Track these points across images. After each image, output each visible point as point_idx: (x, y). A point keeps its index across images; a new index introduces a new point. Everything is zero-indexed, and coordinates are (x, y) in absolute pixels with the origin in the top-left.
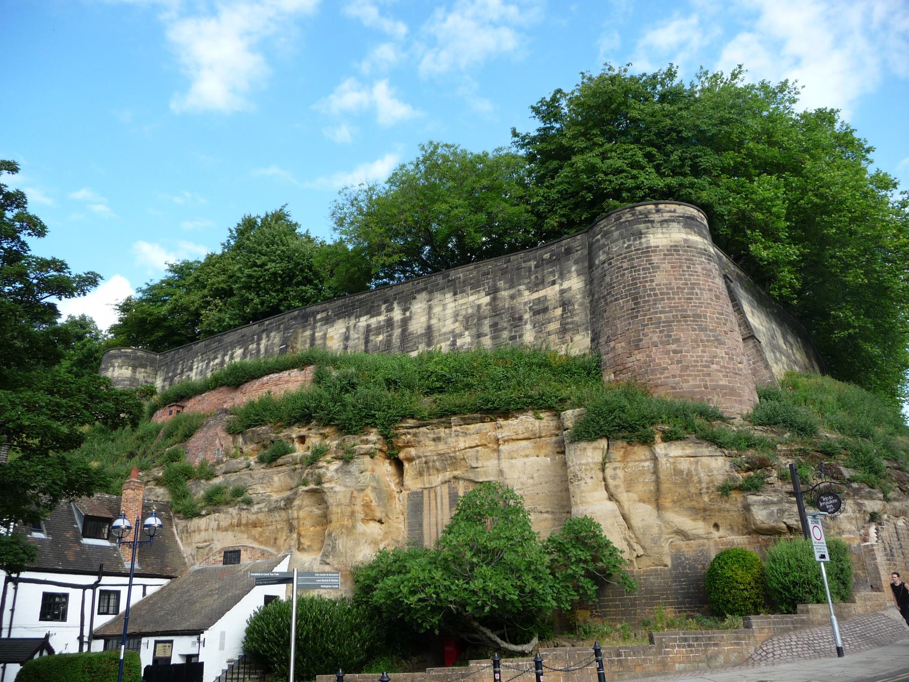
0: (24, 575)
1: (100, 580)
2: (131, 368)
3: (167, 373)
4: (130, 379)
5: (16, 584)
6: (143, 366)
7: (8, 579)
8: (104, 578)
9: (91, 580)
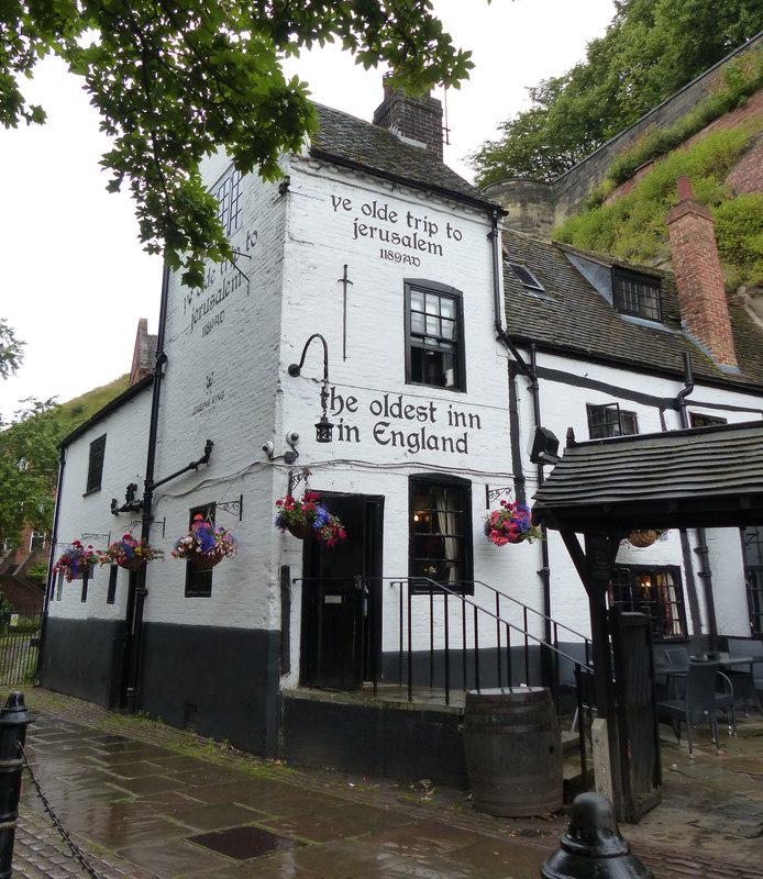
0: (544, 361)
1: (689, 392)
2: (519, 205)
3: (571, 201)
4: (520, 219)
5: (533, 380)
6: (533, 200)
7: (515, 368)
8: (697, 389)
9: (667, 389)
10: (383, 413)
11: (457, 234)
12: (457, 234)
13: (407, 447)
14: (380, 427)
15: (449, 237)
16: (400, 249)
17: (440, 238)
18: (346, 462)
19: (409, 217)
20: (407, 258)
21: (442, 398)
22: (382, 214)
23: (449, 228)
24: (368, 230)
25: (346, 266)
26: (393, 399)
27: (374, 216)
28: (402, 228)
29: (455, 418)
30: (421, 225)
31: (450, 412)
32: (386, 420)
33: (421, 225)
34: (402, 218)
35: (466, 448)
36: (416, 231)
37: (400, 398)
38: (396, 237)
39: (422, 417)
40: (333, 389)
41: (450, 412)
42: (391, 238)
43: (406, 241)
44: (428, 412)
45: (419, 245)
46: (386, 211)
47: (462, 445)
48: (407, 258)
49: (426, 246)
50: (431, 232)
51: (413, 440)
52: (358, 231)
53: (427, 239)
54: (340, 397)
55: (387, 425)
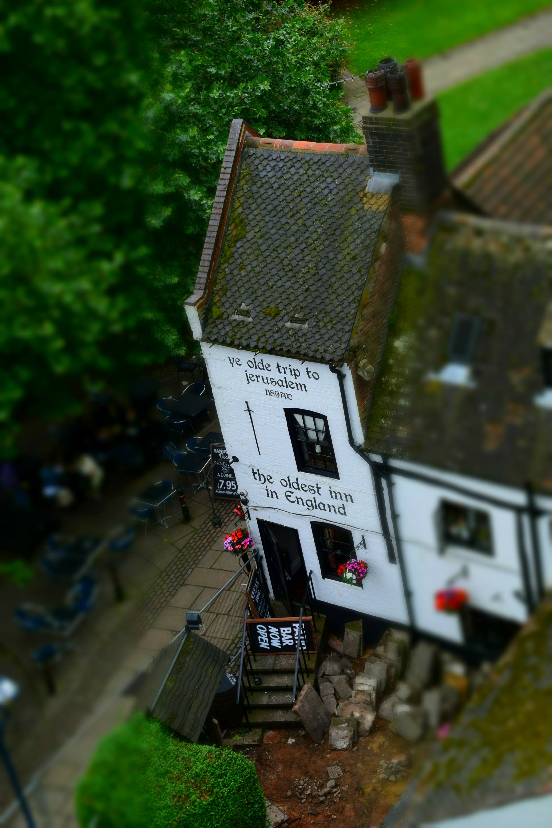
10: (288, 486)
11: (315, 375)
12: (315, 375)
13: (306, 507)
14: (290, 494)
15: (310, 378)
16: (277, 389)
17: (303, 379)
18: (272, 508)
19: (278, 367)
20: (283, 395)
21: (324, 482)
22: (261, 366)
23: (308, 372)
24: (255, 378)
25: (247, 402)
26: (292, 480)
27: (256, 368)
28: (275, 374)
29: (334, 494)
30: (288, 371)
31: (330, 491)
32: (290, 490)
33: (288, 371)
34: (274, 367)
35: (345, 512)
36: (285, 376)
37: (297, 479)
38: (273, 381)
39: (313, 492)
40: (258, 470)
41: (330, 491)
42: (270, 382)
43: (280, 383)
44: (315, 489)
45: (289, 385)
46: (262, 364)
47: (342, 511)
48: (283, 395)
49: (294, 385)
50: (296, 375)
51: (309, 503)
52: (249, 378)
53: (294, 381)
54: (262, 475)
55: (292, 493)
